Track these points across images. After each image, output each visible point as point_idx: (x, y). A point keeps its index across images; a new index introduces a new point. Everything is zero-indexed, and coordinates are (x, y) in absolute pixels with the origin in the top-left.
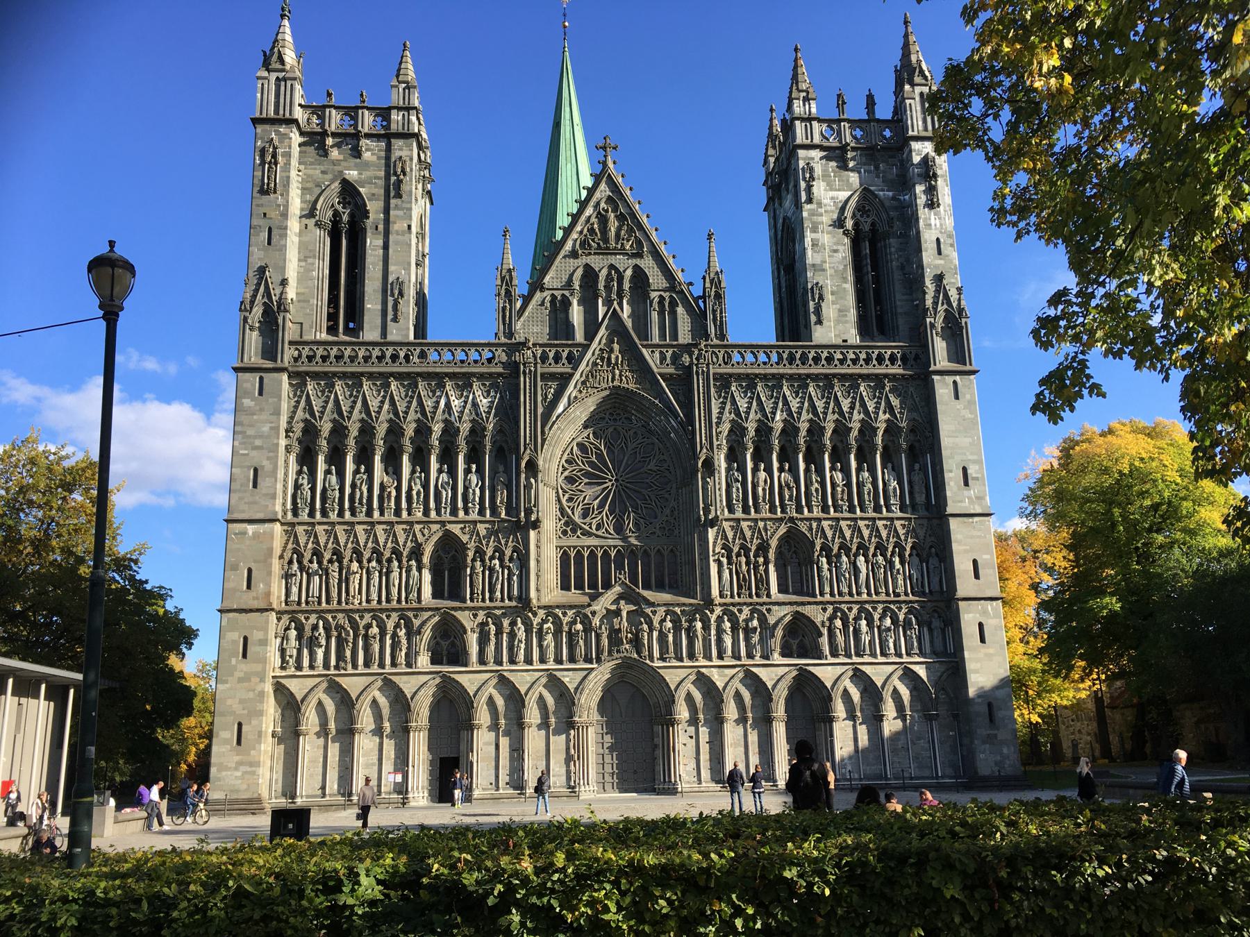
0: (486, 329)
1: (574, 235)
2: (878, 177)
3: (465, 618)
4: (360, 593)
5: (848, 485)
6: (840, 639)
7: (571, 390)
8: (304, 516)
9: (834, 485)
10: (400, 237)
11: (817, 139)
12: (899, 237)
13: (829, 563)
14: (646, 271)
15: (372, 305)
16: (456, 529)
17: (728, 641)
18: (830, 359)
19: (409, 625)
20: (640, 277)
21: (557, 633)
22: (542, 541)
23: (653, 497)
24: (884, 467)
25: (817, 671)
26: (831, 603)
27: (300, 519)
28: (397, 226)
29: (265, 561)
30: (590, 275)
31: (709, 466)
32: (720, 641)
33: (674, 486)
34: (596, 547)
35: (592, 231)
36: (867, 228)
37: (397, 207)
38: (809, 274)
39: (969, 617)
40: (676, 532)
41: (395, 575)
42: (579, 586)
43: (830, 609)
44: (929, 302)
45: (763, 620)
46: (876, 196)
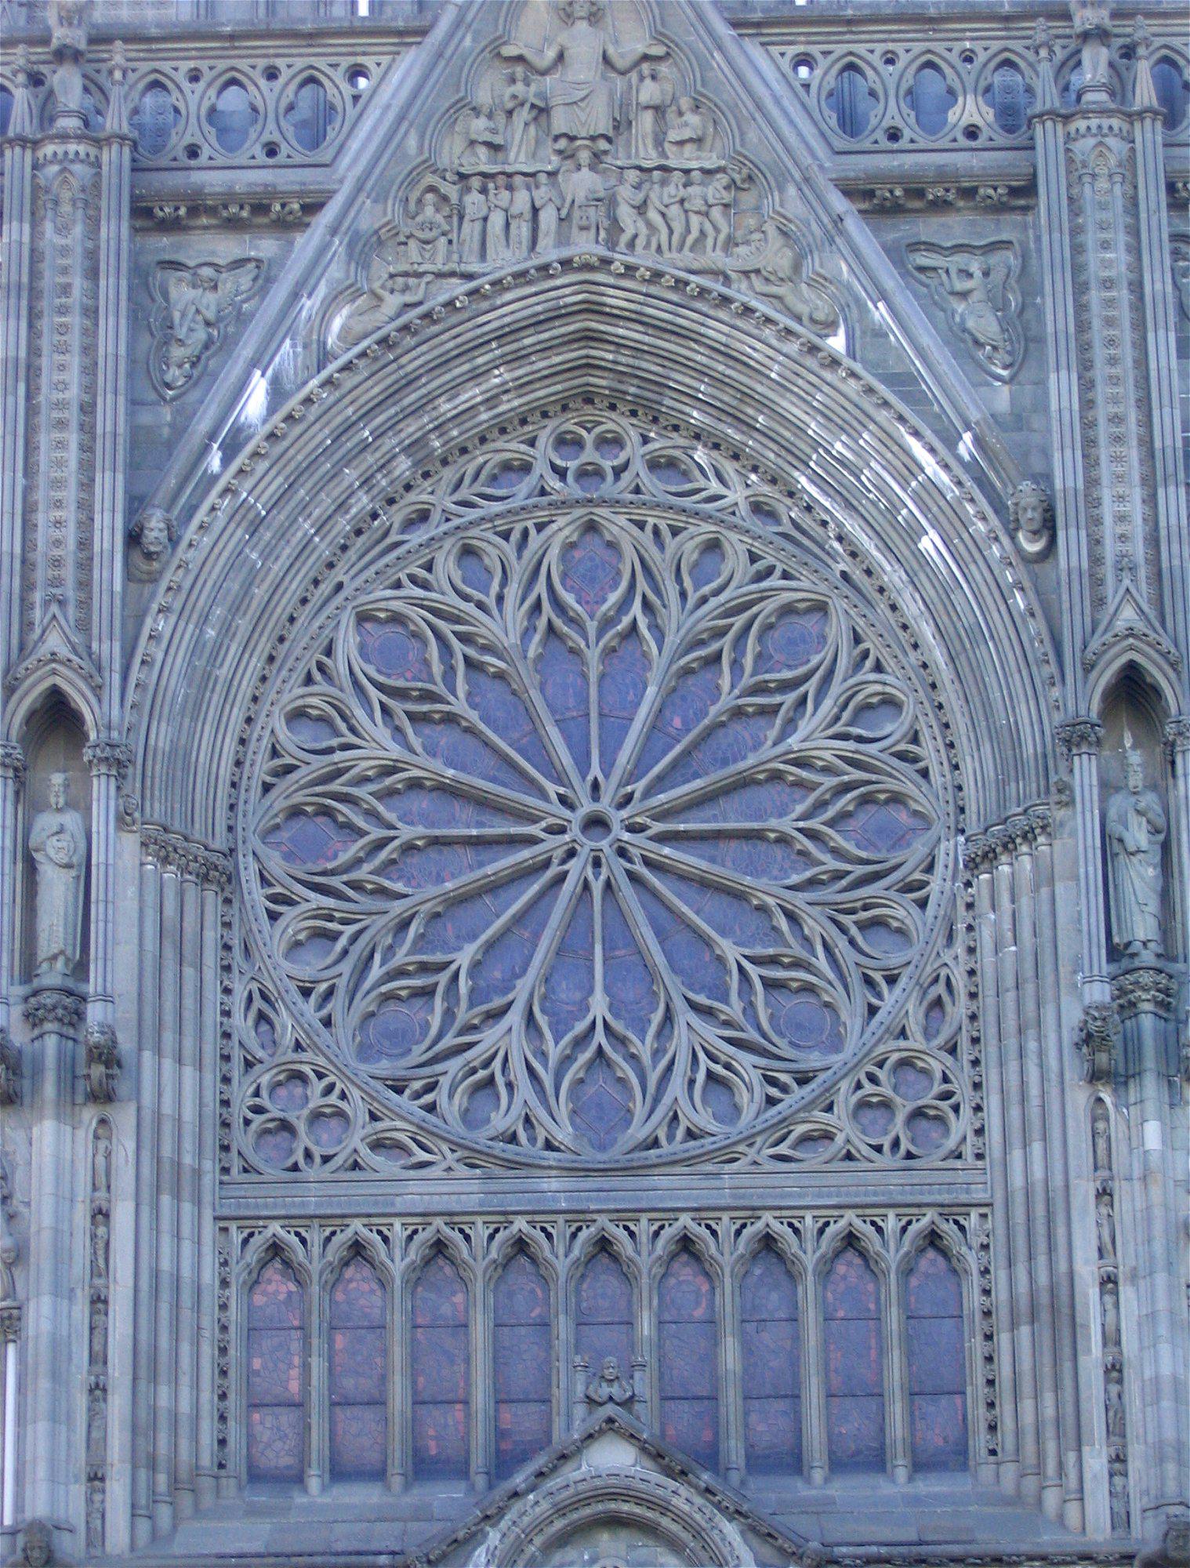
22: (124, 1180)
23: (815, 925)
33: (951, 850)
40: (961, 1126)
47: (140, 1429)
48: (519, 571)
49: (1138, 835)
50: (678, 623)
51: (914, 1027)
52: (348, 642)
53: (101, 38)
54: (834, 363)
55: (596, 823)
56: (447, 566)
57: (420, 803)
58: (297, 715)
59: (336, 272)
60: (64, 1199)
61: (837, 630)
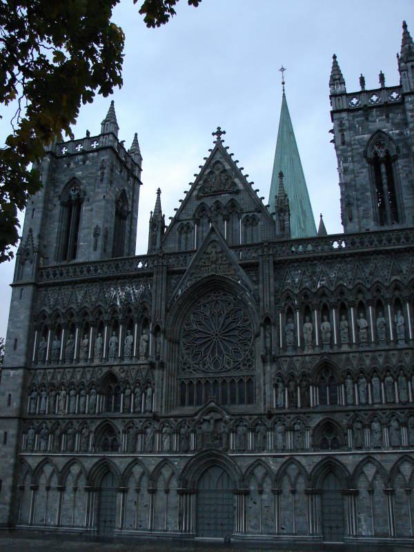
2: (388, 122)
4: (65, 409)
5: (368, 328)
9: (358, 328)
10: (100, 203)
12: (403, 158)
13: (354, 383)
14: (239, 202)
16: (116, 370)
23: (239, 344)
24: (394, 313)
25: (340, 458)
26: (354, 411)
27: (39, 366)
29: (17, 391)
32: (276, 438)
34: (201, 378)
36: (382, 155)
37: (98, 187)
41: (82, 399)
43: (352, 414)
46: (387, 134)
47: (167, 401)
48: (209, 307)
49: (268, 335)
50: (226, 312)
51: (249, 355)
52: (192, 316)
53: (164, 255)
54: (238, 284)
55: (217, 335)
56: (202, 308)
57: (199, 333)
58: (187, 325)
59: (188, 278)
60: (159, 377)
61: (242, 312)
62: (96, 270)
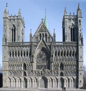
0: (29, 41)
1: (39, 30)
3: (26, 72)
5: (68, 58)
6: (66, 74)
7: (37, 47)
8: (10, 61)
11: (67, 18)
15: (16, 38)
17: (54, 74)
18: (67, 44)
19: (21, 72)
20: (46, 34)
21: (36, 73)
28: (19, 29)
30: (40, 34)
31: (52, 56)
35: (41, 29)
38: (65, 34)
39: (80, 72)
41: (19, 67)
42: (38, 69)
44: (79, 37)
45: (58, 72)
62: (20, 44)
